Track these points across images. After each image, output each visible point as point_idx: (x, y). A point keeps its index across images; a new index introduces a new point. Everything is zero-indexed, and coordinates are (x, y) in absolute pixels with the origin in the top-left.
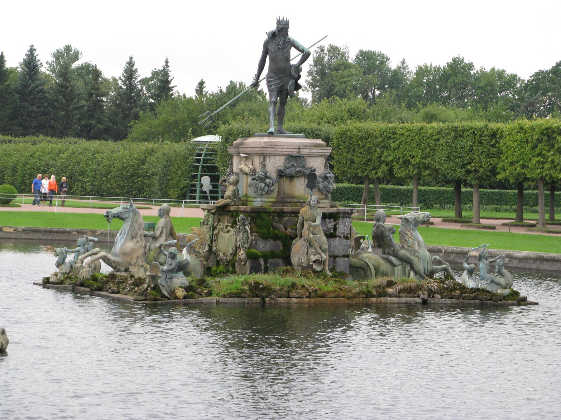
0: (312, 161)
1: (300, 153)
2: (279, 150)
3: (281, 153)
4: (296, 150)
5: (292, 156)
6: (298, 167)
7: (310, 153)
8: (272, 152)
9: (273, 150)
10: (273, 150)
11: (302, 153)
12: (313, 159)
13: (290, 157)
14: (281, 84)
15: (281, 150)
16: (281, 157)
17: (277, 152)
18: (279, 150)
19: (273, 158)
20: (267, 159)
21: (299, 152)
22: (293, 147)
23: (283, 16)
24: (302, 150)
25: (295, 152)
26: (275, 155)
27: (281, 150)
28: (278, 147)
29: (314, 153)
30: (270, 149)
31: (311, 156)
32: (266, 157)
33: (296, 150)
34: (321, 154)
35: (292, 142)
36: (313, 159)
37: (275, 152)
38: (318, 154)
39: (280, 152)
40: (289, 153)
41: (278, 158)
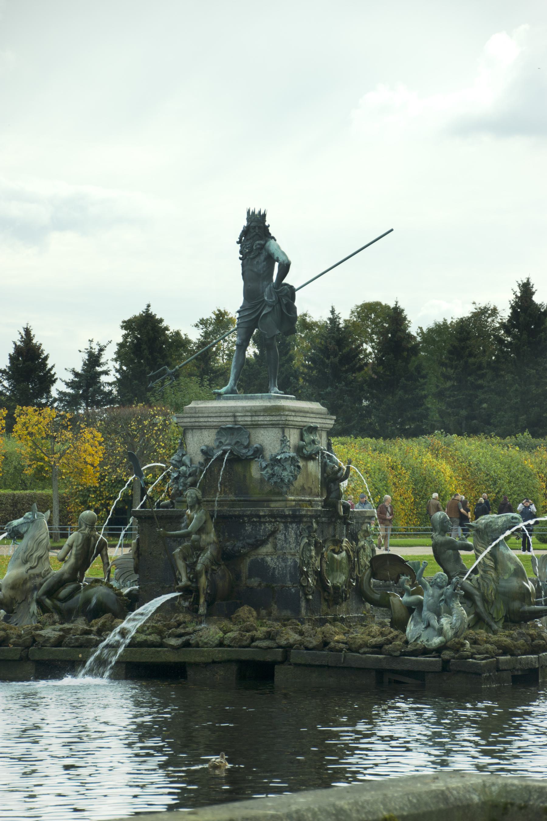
0: (260, 435)
1: (237, 423)
2: (202, 419)
3: (208, 424)
4: (229, 419)
5: (222, 428)
6: (227, 445)
7: (254, 423)
8: (193, 424)
9: (193, 420)
10: (193, 420)
11: (241, 423)
12: (262, 431)
13: (222, 431)
14: (253, 317)
15: (206, 420)
16: (211, 430)
17: (200, 424)
18: (202, 419)
19: (197, 433)
20: (189, 436)
21: (235, 421)
22: (223, 414)
23: (257, 208)
24: (239, 419)
25: (228, 422)
26: (200, 428)
27: (206, 420)
28: (200, 415)
29: (259, 423)
30: (188, 420)
31: (256, 426)
32: (187, 431)
33: (229, 419)
34: (271, 422)
35: (228, 407)
36: (262, 432)
37: (197, 424)
38: (266, 422)
39: (204, 424)
40: (220, 424)
41: (206, 433)
